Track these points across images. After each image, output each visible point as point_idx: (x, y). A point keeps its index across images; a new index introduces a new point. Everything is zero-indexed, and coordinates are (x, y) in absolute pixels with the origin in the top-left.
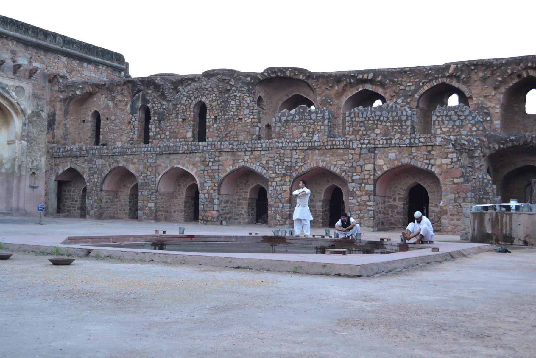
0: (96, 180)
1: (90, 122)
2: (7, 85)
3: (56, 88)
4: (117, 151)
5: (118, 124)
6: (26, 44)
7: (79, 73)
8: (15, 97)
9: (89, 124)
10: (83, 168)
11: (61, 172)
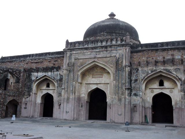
2: (170, 69)
6: (179, 49)
8: (175, 74)
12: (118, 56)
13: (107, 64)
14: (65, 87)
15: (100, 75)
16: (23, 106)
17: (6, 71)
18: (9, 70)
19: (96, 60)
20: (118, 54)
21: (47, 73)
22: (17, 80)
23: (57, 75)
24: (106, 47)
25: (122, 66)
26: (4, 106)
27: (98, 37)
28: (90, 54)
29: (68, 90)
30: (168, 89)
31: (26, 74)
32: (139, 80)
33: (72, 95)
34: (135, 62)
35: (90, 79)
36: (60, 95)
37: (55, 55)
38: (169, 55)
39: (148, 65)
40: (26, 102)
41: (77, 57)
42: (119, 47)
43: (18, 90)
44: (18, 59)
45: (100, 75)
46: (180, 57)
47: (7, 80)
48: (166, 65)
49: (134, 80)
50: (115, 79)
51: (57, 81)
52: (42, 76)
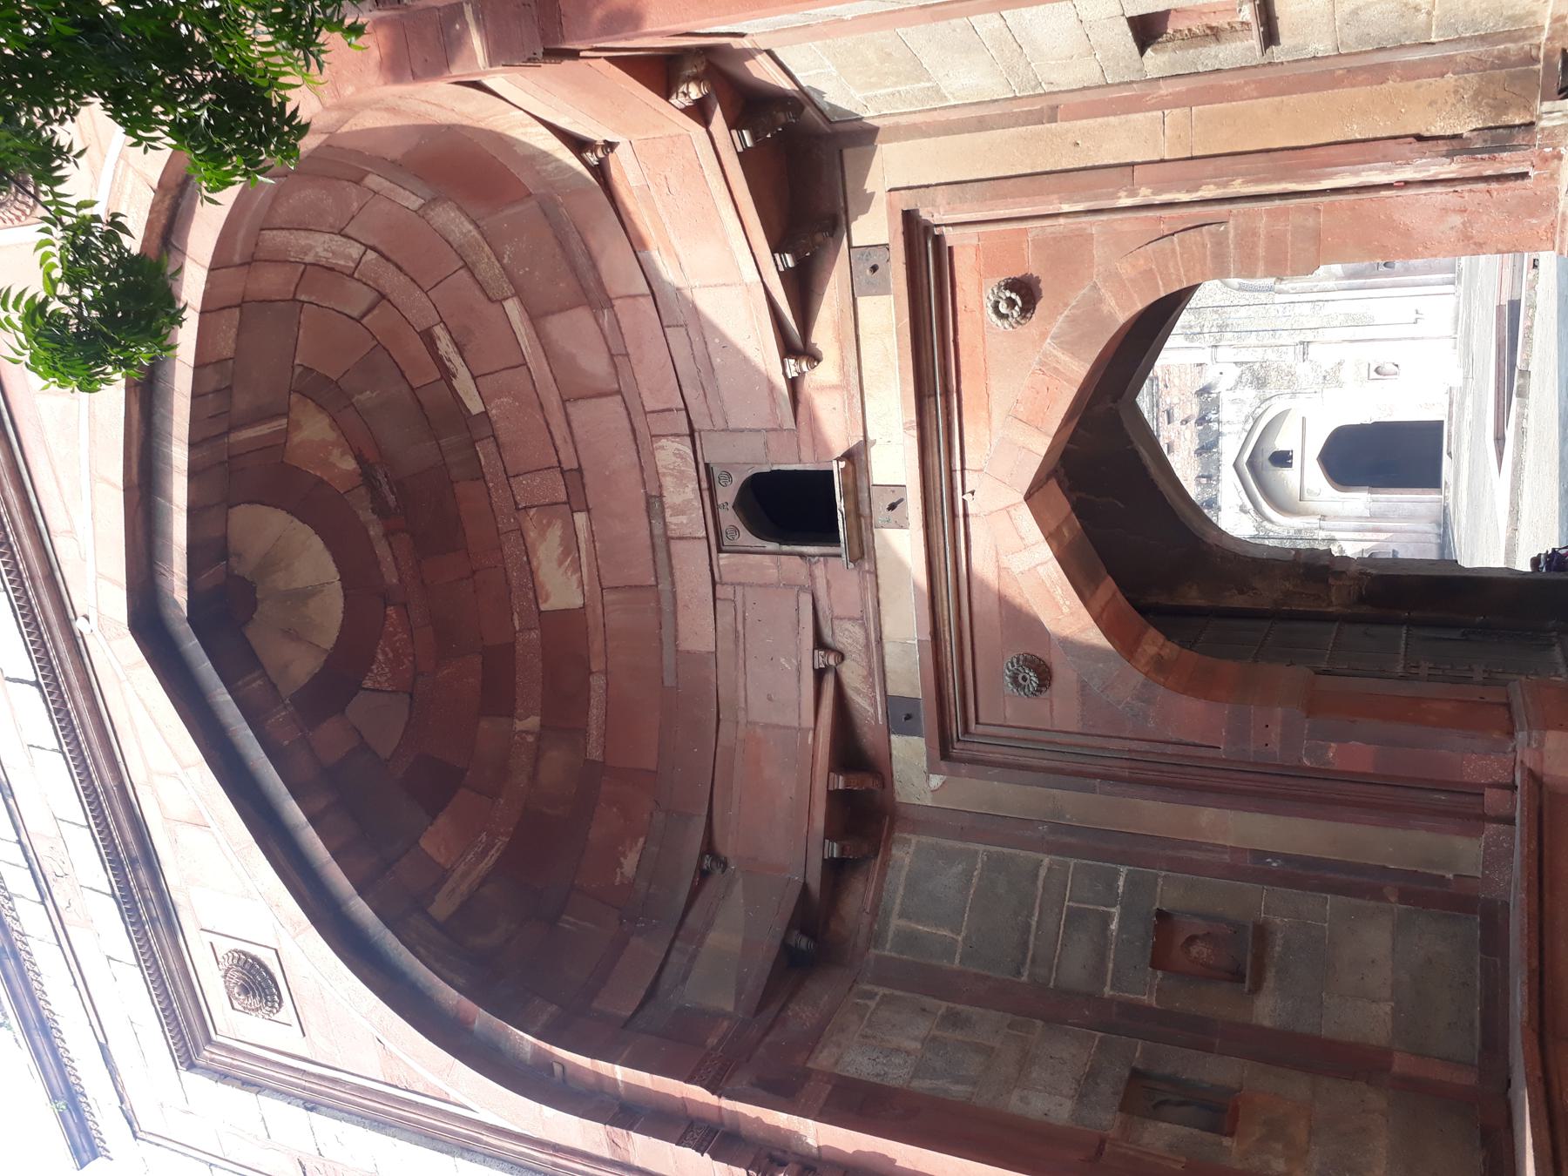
23: (1234, 401)
36: (1329, 378)
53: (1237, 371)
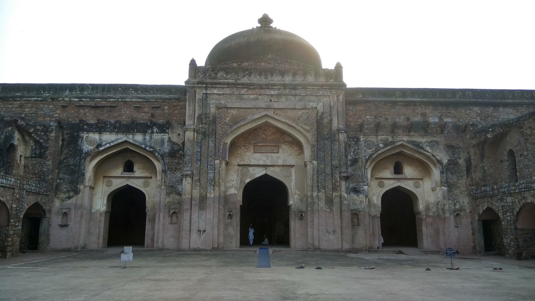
0: (509, 218)
1: (508, 161)
3: (468, 136)
4: (523, 187)
5: (531, 158)
6: (435, 105)
7: (495, 118)
8: (430, 151)
9: (506, 163)
10: (498, 207)
11: (481, 212)
12: (320, 107)
13: (297, 124)
14: (194, 172)
15: (273, 146)
16: (56, 220)
17: (9, 123)
18: (16, 121)
19: (270, 113)
20: (322, 104)
21: (131, 136)
22: (35, 149)
23: (163, 141)
24: (294, 87)
25: (331, 130)
26: (19, 222)
27: (263, 64)
28: (257, 99)
29: (203, 180)
30: (410, 179)
31: (63, 135)
32: (360, 160)
33: (212, 192)
34: (352, 124)
35: (247, 153)
36: (173, 189)
37: (153, 94)
38: (418, 114)
39: (377, 131)
40: (64, 211)
41: (223, 102)
42: (323, 89)
43: (43, 177)
44: (32, 94)
45: (273, 146)
46: (437, 120)
47: (12, 148)
48: (412, 133)
49: (351, 160)
50: (316, 156)
51: (162, 156)
52: (116, 143)
53: (180, 143)
